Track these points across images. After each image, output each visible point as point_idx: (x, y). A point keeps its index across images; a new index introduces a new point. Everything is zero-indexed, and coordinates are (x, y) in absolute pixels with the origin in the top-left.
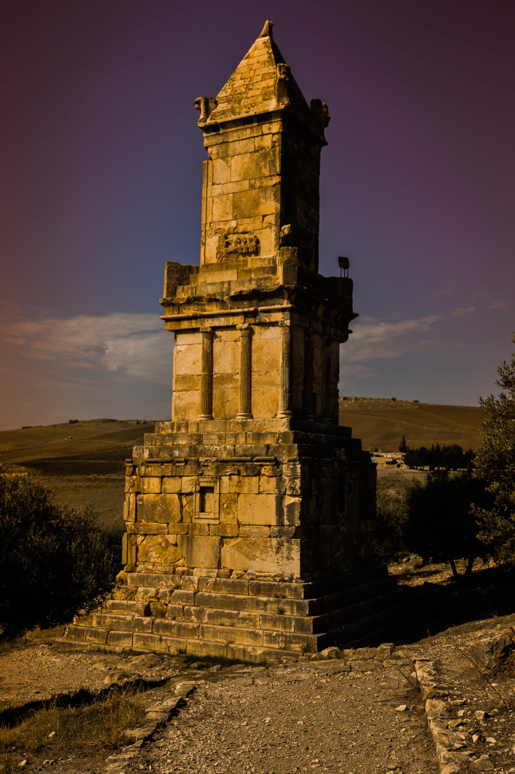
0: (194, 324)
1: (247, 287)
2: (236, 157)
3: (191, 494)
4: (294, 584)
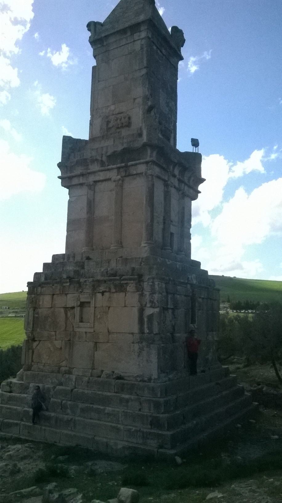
0: (81, 180)
1: (120, 148)
3: (73, 308)
4: (152, 384)
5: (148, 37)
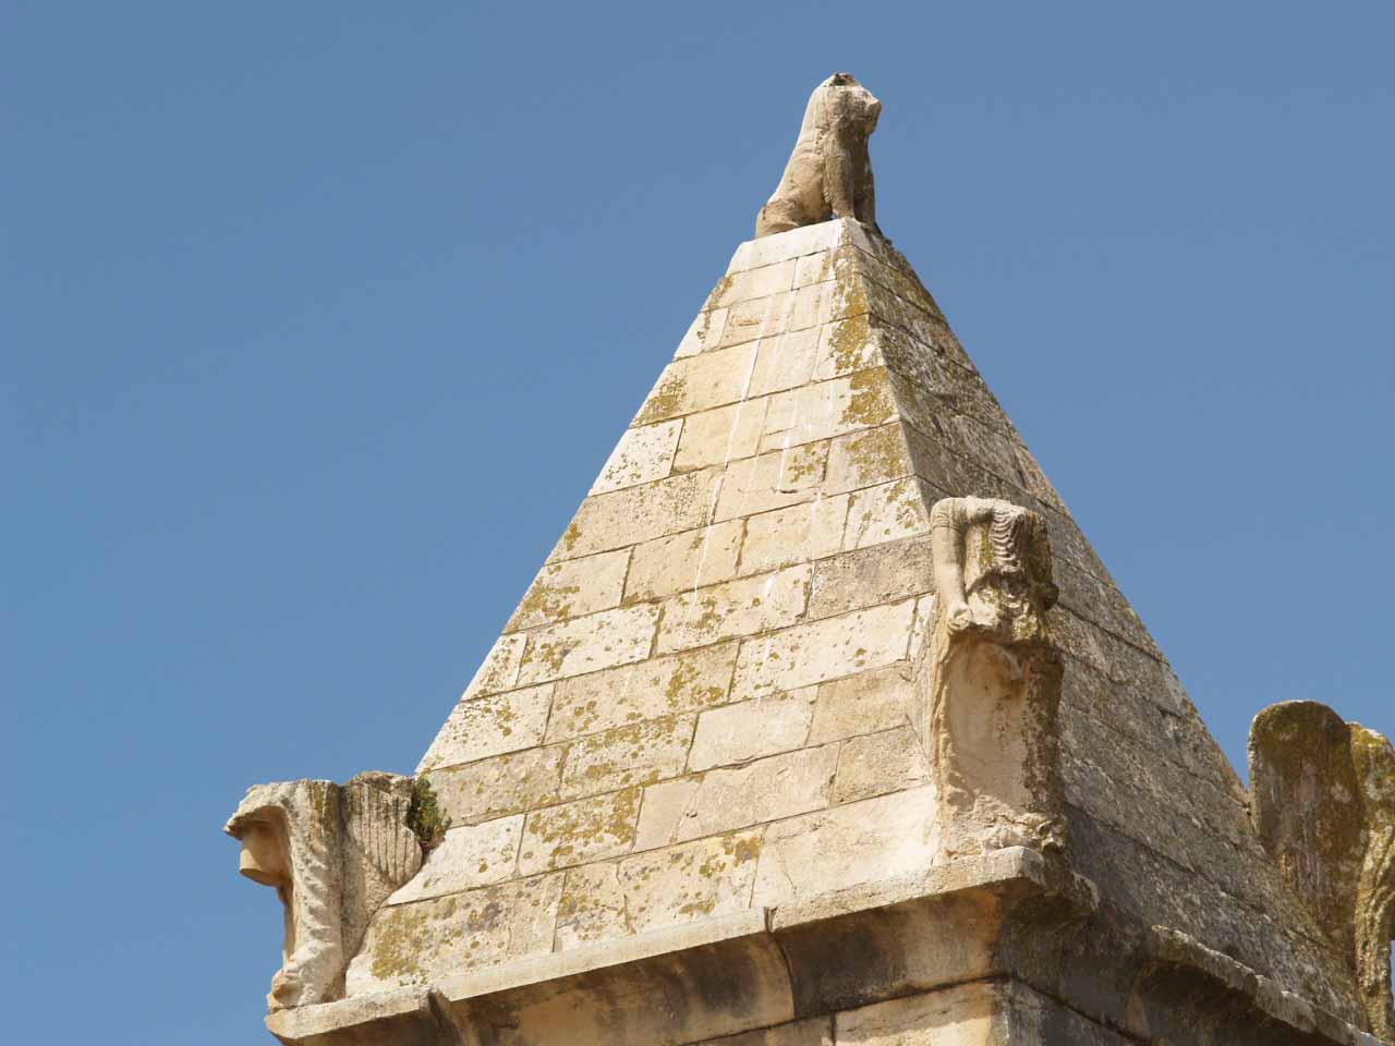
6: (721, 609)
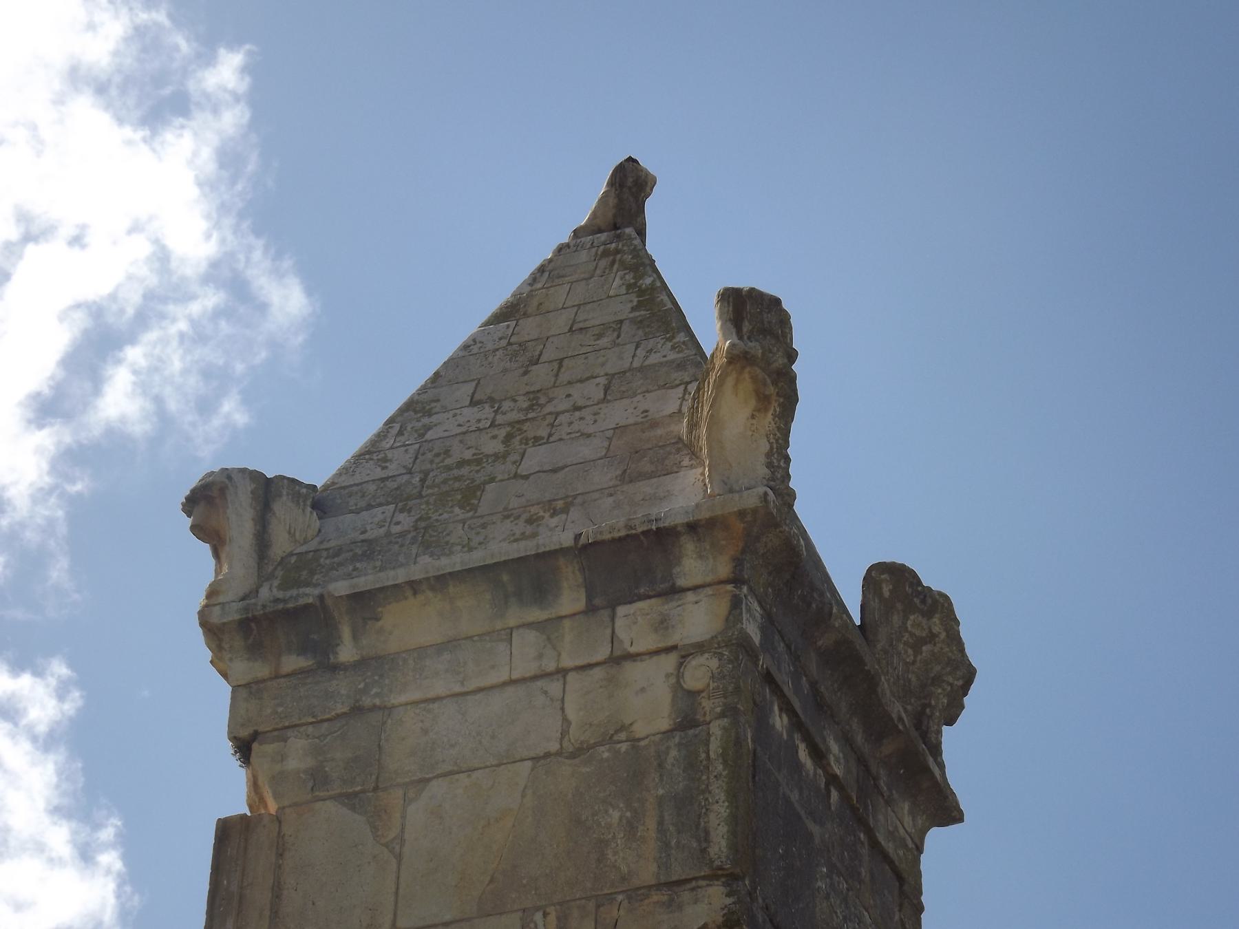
2: (438, 788)
5: (744, 644)
6: (542, 400)
